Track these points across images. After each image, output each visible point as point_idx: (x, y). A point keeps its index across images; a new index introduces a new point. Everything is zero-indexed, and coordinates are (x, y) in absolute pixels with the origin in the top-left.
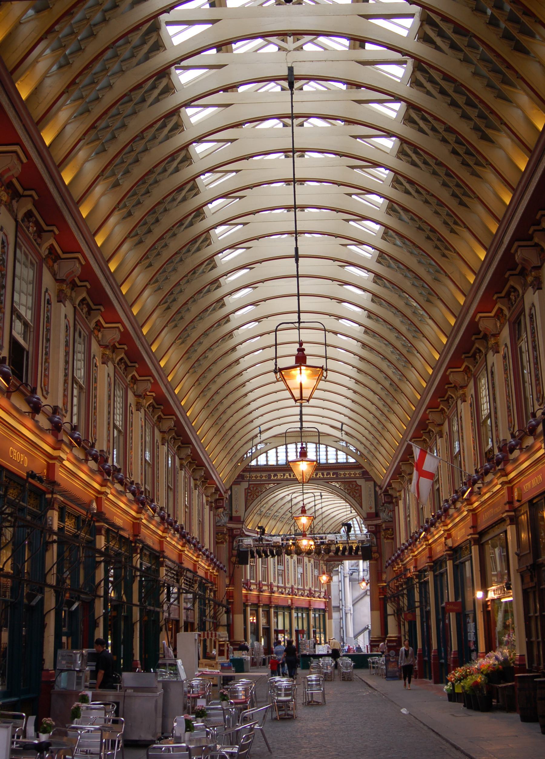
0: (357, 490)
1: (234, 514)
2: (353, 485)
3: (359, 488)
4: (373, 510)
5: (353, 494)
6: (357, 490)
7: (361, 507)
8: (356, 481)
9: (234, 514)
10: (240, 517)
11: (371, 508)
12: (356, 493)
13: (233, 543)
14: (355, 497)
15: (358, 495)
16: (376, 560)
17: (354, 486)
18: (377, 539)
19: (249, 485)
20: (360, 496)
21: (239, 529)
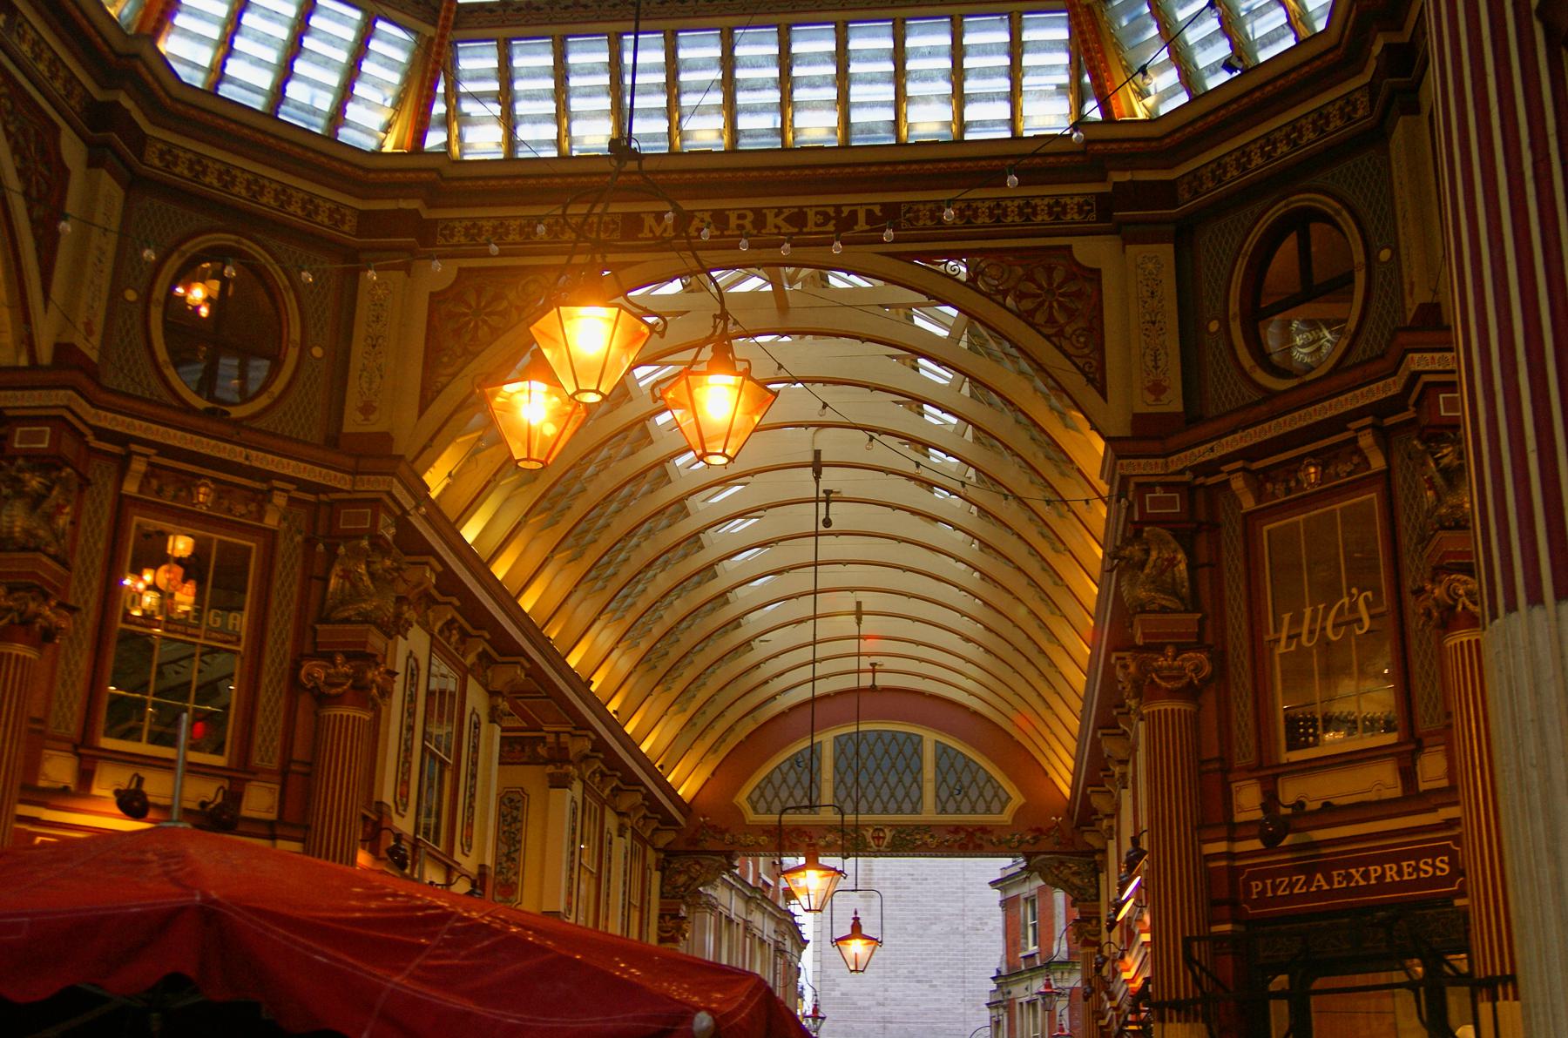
0: (1078, 295)
1: (353, 422)
2: (1050, 270)
3: (1089, 289)
4: (1173, 403)
5: (1051, 320)
6: (1078, 295)
7: (1103, 393)
8: (1069, 248)
9: (353, 422)
10: (386, 438)
11: (1157, 389)
12: (1071, 314)
13: (326, 581)
14: (1060, 333)
15: (1081, 323)
16: (1190, 692)
17: (1058, 276)
18: (1191, 567)
19: (460, 270)
20: (1095, 330)
21: (375, 503)
